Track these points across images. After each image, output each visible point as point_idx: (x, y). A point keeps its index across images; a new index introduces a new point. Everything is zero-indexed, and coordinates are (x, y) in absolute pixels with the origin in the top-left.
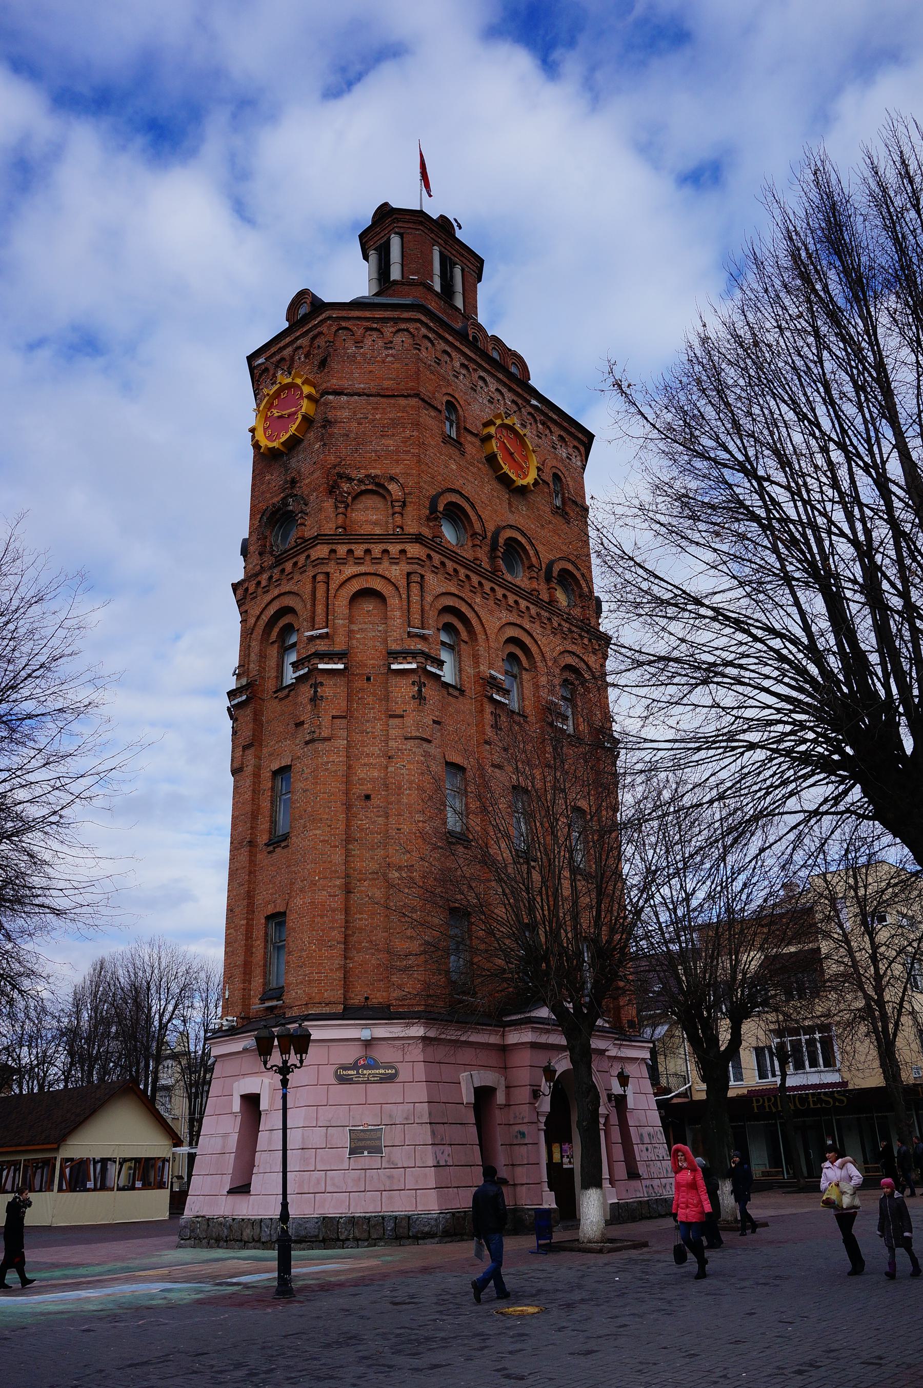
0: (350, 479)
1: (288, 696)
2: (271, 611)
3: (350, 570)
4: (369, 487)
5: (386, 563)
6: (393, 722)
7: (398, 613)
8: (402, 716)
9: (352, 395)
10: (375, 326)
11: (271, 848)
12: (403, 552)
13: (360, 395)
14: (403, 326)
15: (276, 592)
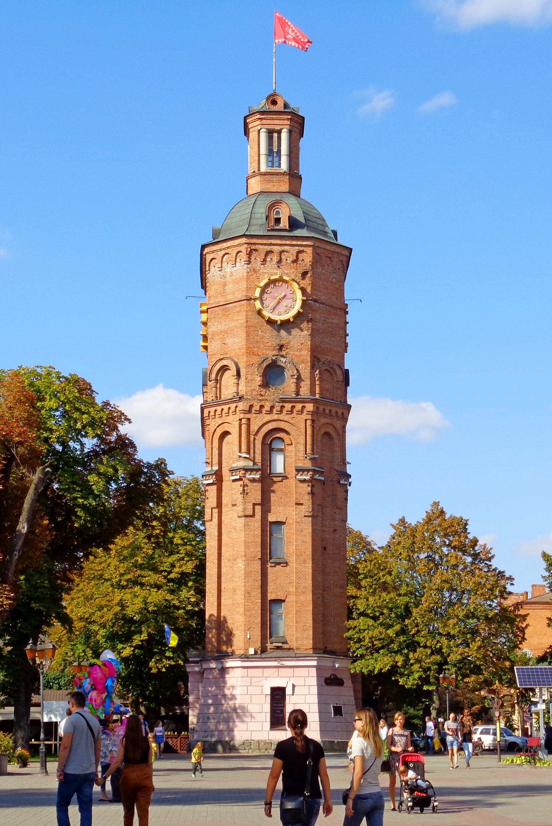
0: (319, 360)
1: (282, 481)
2: (271, 426)
3: (323, 420)
4: (327, 368)
5: (335, 421)
6: (337, 511)
7: (338, 449)
8: (341, 509)
9: (321, 303)
10: (330, 255)
11: (273, 565)
12: (343, 414)
13: (323, 304)
14: (341, 258)
15: (275, 417)
